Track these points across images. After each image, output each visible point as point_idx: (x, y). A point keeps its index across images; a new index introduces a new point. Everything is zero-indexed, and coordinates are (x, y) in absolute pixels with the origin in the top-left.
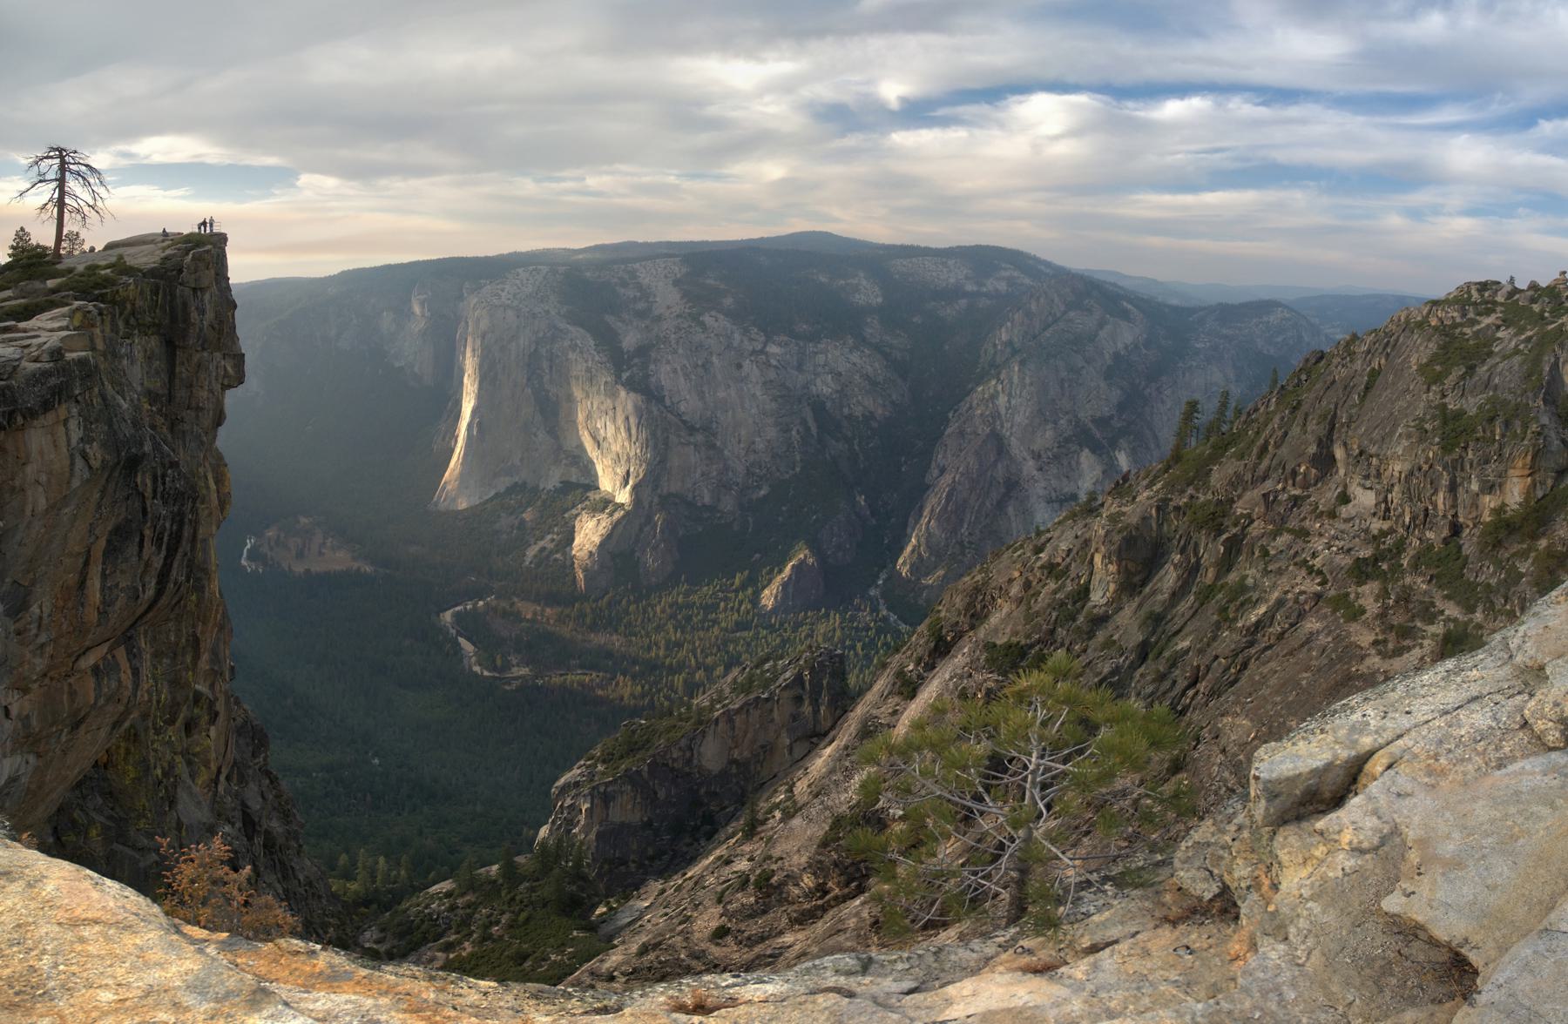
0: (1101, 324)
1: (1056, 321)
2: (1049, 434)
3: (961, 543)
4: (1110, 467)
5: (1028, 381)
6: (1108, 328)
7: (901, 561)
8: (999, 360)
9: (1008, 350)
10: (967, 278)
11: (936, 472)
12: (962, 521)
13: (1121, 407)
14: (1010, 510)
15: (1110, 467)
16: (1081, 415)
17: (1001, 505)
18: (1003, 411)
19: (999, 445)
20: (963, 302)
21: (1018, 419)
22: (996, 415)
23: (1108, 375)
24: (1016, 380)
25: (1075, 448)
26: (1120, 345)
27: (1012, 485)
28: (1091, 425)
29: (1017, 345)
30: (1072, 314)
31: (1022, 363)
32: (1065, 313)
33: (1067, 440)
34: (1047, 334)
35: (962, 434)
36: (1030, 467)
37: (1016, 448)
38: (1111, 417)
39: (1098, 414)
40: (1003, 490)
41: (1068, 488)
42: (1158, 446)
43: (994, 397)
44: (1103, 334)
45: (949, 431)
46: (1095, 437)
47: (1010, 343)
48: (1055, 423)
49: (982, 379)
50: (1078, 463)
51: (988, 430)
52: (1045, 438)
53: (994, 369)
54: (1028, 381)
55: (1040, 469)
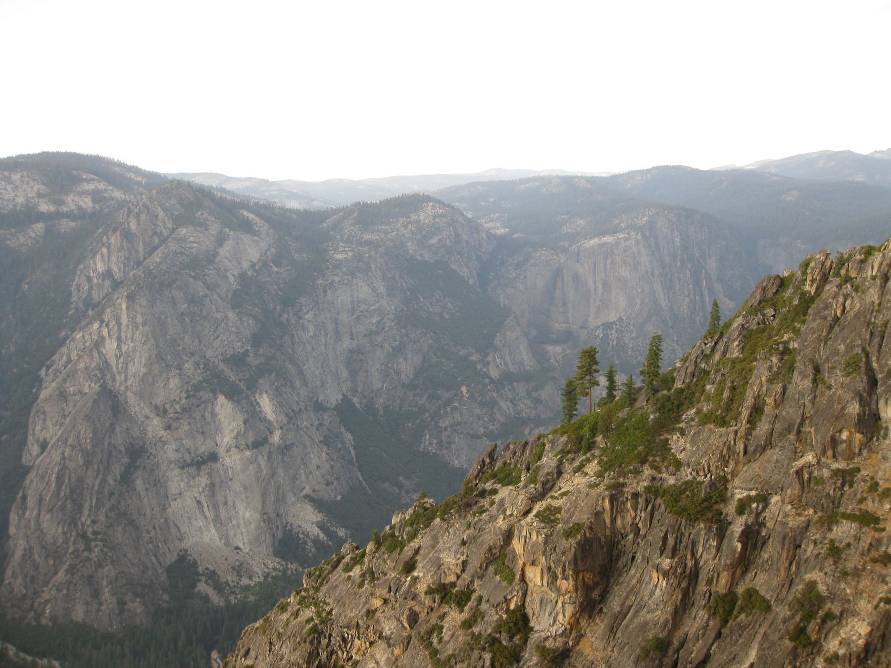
0: (220, 241)
1: (164, 241)
2: (174, 383)
3: (83, 536)
4: (253, 415)
5: (140, 320)
6: (229, 245)
7: (9, 573)
8: (96, 296)
9: (107, 283)
10: (40, 195)
11: (35, 450)
12: (79, 508)
13: (256, 340)
14: (139, 484)
15: (253, 415)
16: (209, 354)
17: (126, 479)
18: (113, 362)
19: (111, 402)
20: (40, 227)
21: (132, 369)
22: (105, 367)
23: (237, 302)
24: (124, 320)
25: (205, 395)
26: (246, 265)
27: (137, 453)
28: (222, 366)
29: (118, 276)
30: (183, 231)
31: (131, 298)
32: (174, 230)
33: (198, 388)
34: (157, 257)
35: (62, 395)
36: (155, 427)
37: (135, 405)
38: (246, 353)
39: (230, 352)
40: (126, 460)
41: (204, 447)
42: (305, 383)
43: (99, 344)
44: (224, 251)
45: (44, 394)
46: (234, 380)
47: (108, 274)
48: (179, 368)
49: (78, 321)
50: (214, 415)
51: (96, 387)
52: (171, 388)
53: (94, 308)
54: (140, 320)
55: (168, 427)
